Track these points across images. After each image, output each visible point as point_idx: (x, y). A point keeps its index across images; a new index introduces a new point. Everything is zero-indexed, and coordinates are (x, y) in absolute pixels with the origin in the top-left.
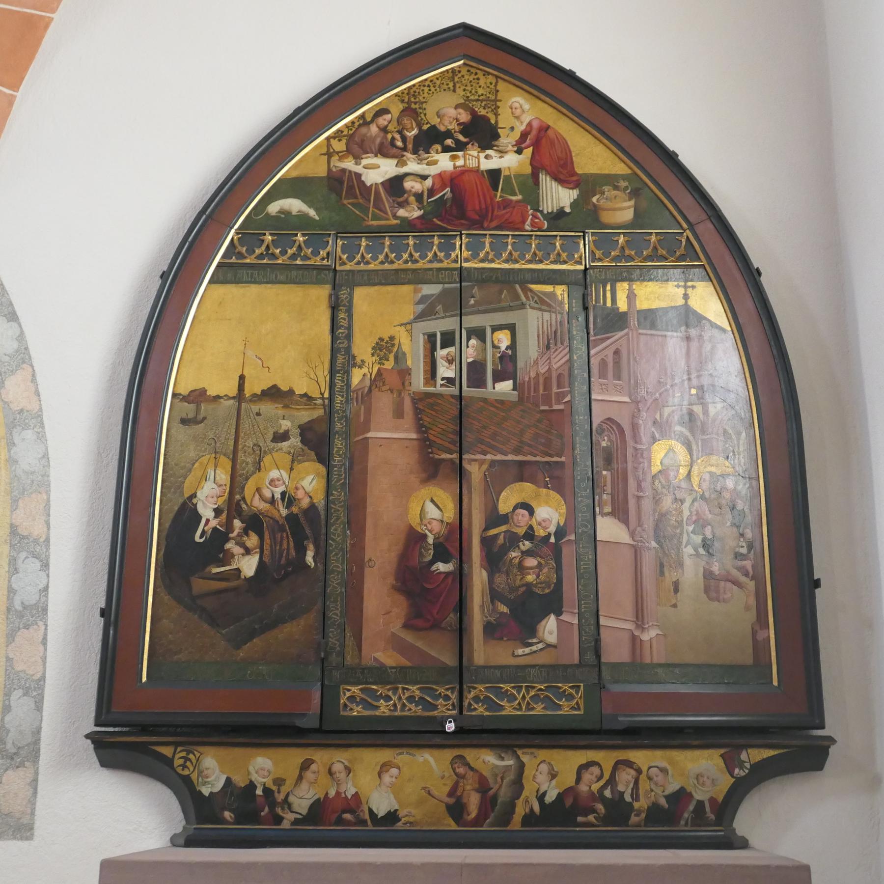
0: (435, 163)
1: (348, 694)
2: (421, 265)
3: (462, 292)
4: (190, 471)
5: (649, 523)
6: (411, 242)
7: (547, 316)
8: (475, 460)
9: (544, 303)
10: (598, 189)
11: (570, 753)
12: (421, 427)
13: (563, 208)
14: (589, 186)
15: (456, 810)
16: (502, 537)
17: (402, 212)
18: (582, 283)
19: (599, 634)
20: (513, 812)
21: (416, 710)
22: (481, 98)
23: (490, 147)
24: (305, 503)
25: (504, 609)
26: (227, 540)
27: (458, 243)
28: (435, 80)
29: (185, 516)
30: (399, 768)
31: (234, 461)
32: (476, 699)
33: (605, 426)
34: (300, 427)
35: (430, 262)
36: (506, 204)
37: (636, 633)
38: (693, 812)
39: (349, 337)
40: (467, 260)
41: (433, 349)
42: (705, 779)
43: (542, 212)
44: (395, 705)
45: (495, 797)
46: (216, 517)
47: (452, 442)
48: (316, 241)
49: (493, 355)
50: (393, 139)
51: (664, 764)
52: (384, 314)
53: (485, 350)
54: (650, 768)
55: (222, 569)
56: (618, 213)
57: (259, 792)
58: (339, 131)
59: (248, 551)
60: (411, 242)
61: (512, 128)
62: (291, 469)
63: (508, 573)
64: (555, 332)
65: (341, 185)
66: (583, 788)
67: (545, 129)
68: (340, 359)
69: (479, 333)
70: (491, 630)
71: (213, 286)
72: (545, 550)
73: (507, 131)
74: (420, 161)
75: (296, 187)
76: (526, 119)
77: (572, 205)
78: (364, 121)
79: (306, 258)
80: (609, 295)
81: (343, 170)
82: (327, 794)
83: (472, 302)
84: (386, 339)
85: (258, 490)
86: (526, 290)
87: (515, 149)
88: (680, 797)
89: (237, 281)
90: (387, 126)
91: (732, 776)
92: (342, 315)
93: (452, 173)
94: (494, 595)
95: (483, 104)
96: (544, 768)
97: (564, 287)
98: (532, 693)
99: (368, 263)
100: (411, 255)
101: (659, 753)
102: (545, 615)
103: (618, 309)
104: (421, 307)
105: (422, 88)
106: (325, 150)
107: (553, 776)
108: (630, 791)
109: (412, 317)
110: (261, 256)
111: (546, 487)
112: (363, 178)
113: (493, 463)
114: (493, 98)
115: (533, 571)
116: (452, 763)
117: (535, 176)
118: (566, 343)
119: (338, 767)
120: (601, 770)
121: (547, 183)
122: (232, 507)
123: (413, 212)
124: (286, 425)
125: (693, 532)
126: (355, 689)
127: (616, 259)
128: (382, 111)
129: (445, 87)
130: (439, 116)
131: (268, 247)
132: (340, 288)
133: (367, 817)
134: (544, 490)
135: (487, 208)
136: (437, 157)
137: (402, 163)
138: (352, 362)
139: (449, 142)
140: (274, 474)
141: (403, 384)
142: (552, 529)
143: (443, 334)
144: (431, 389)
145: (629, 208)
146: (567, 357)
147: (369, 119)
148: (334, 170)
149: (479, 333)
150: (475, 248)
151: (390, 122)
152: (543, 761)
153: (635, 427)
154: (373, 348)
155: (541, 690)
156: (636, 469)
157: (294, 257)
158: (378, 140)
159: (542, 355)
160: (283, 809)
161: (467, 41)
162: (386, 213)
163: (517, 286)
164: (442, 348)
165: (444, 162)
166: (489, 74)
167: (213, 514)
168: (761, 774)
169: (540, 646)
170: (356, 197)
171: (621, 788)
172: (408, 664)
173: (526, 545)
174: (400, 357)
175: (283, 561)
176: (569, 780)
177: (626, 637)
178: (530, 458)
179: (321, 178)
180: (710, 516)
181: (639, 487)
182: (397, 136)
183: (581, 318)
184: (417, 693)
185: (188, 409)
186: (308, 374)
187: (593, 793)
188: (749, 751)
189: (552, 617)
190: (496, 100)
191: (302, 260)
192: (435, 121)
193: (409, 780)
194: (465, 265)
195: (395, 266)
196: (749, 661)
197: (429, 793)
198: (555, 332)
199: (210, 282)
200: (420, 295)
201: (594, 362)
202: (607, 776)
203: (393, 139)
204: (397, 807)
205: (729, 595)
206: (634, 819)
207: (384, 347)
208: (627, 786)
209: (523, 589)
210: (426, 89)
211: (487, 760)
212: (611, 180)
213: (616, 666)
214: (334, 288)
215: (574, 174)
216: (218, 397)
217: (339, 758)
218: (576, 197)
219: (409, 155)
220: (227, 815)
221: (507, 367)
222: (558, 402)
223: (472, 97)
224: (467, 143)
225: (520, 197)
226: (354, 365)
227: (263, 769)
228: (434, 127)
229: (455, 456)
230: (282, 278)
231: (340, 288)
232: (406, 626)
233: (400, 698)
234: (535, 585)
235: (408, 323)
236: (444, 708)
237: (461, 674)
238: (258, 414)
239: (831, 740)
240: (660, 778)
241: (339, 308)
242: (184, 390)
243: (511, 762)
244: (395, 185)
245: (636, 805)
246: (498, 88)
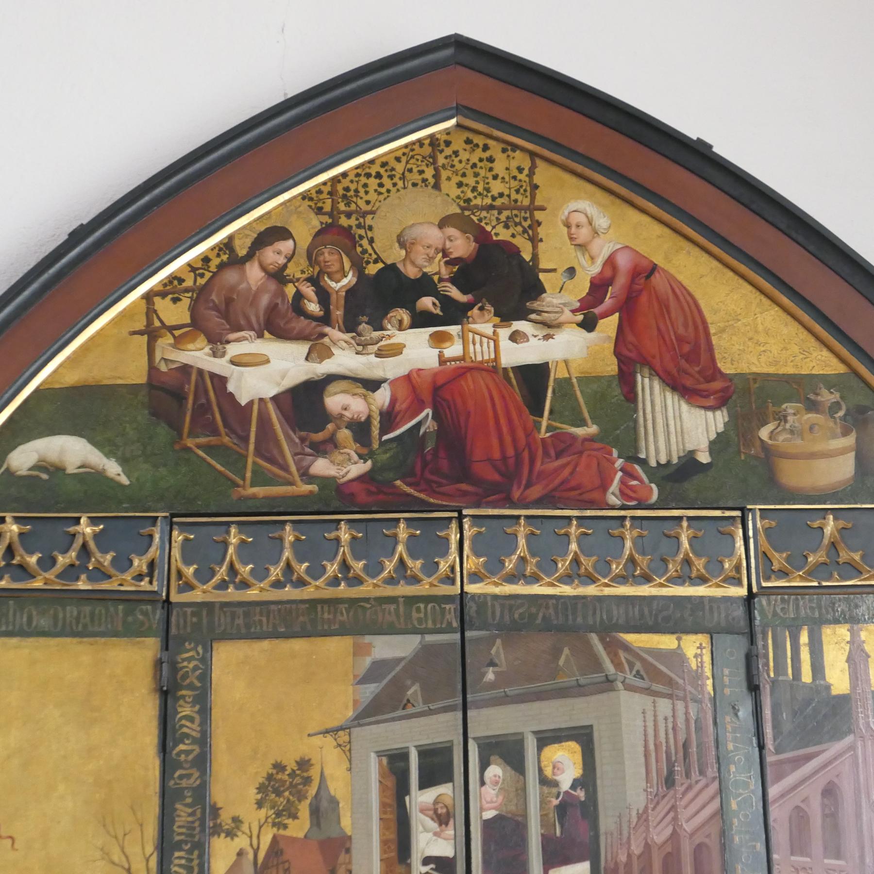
0: (396, 350)
2: (368, 589)
6: (345, 534)
7: (664, 706)
9: (659, 677)
10: (771, 408)
13: (692, 453)
14: (750, 400)
17: (321, 466)
22: (498, 202)
23: (522, 314)
27: (454, 538)
28: (393, 163)
35: (391, 581)
36: (563, 445)
39: (202, 762)
40: (476, 577)
41: (402, 789)
43: (644, 463)
49: (543, 802)
50: (299, 296)
53: (522, 791)
56: (821, 464)
58: (174, 278)
60: (345, 534)
61: (571, 272)
64: (686, 746)
65: (179, 405)
67: (645, 272)
68: (183, 814)
69: (507, 750)
74: (362, 346)
75: (75, 408)
76: (603, 249)
78: (231, 257)
79: (101, 574)
80: (805, 655)
81: (185, 369)
83: (490, 676)
84: (291, 765)
86: (614, 647)
87: (580, 317)
90: (285, 266)
92: (186, 710)
93: (436, 375)
95: (503, 217)
97: (703, 639)
99: (245, 585)
100: (345, 566)
103: (828, 687)
104: (371, 690)
105: (363, 180)
106: (141, 324)
109: (350, 714)
112: (231, 387)
114: (526, 202)
117: (626, 378)
118: (712, 772)
121: (653, 394)
123: (347, 466)
128: (273, 234)
129: (416, 177)
130: (402, 245)
132: (178, 645)
135: (518, 456)
137: (319, 351)
138: (210, 822)
139: (427, 303)
143: (425, 753)
145: (843, 452)
146: (715, 804)
147: (242, 252)
148: (163, 368)
149: (507, 750)
151: (290, 259)
154: (261, 789)
157: (71, 572)
158: (265, 300)
159: (657, 799)
162: (285, 468)
163: (594, 638)
164: (424, 784)
165: (417, 350)
166: (515, 147)
170: (215, 432)
174: (323, 811)
179: (134, 389)
182: (309, 290)
183: (745, 711)
186: (106, 854)
190: (532, 208)
191: (90, 579)
192: (395, 255)
194: (472, 588)
195: (308, 593)
198: (686, 746)
200: (368, 661)
203: (299, 296)
207: (285, 786)
210: (373, 183)
212: (800, 388)
214: (166, 647)
215: (715, 373)
218: (721, 428)
223: (478, 201)
224: (470, 306)
225: (592, 429)
226: (217, 830)
228: (392, 269)
230: (44, 623)
231: (178, 645)
235: (341, 728)
241: (177, 693)
244: (304, 403)
246: (537, 180)
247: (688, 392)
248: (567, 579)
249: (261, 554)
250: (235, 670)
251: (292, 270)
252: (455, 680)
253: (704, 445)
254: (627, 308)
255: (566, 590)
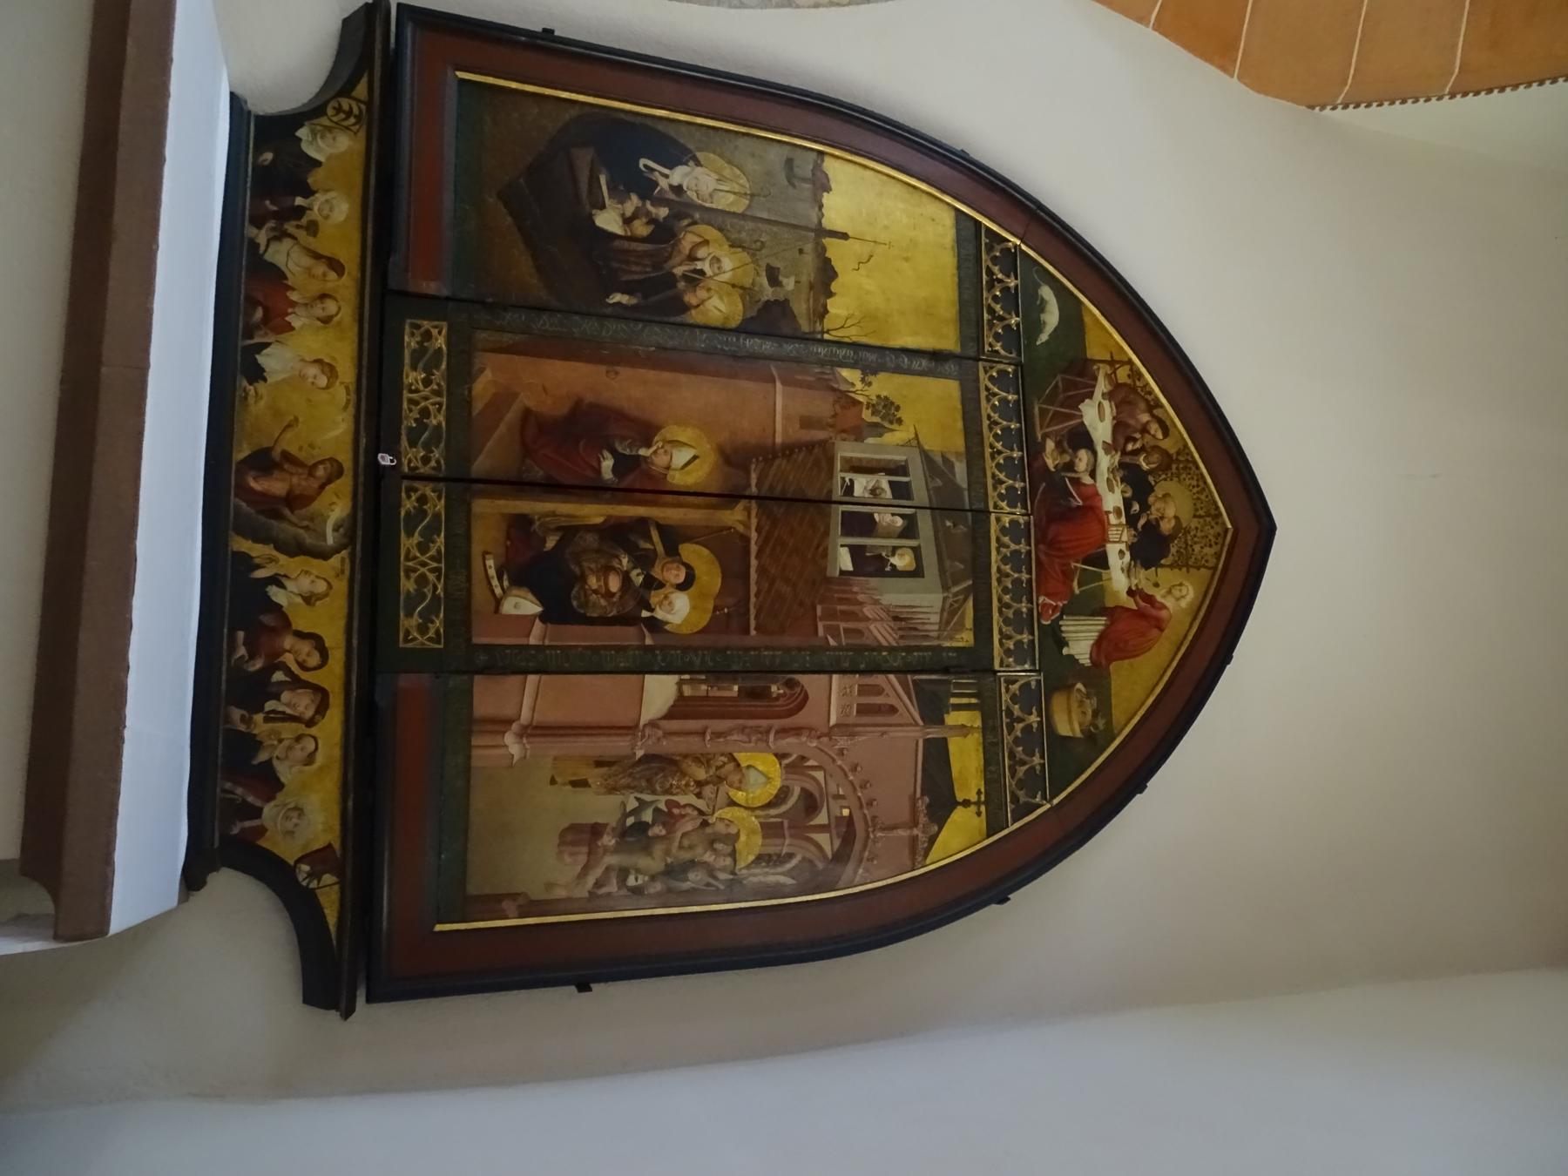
0: (1111, 489)
1: (435, 332)
2: (990, 466)
3: (959, 514)
4: (730, 162)
5: (668, 746)
7: (935, 618)
8: (749, 516)
9: (950, 613)
11: (342, 623)
12: (789, 450)
13: (1067, 644)
14: (1096, 676)
15: (264, 461)
16: (648, 546)
18: (975, 663)
19: (514, 673)
20: (256, 541)
21: (410, 420)
24: (690, 298)
25: (551, 543)
26: (643, 198)
29: (675, 154)
30: (327, 387)
31: (743, 216)
32: (423, 500)
33: (798, 690)
34: (787, 301)
35: (994, 476)
36: (1067, 575)
37: (515, 726)
38: (244, 801)
39: (898, 370)
40: (998, 520)
41: (889, 472)
42: (295, 820)
43: (1061, 618)
44: (417, 391)
45: (279, 516)
46: (671, 187)
47: (772, 488)
48: (1011, 338)
50: (1135, 440)
51: (320, 759)
52: (928, 413)
54: (315, 739)
55: (604, 188)
57: (299, 201)
58: (1140, 375)
59: (627, 221)
61: (1156, 585)
62: (734, 286)
63: (598, 551)
66: (288, 642)
68: (872, 357)
69: (909, 531)
70: (520, 525)
71: (953, 214)
72: (631, 604)
73: (1153, 579)
74: (1112, 471)
76: (1169, 602)
77: (1071, 657)
80: (965, 701)
82: (293, 289)
84: (899, 415)
85: (706, 242)
88: (270, 784)
89: (960, 241)
91: (300, 860)
92: (924, 363)
93: (1100, 508)
94: (570, 532)
96: (321, 587)
98: (431, 577)
99: (988, 400)
100: (999, 452)
101: (337, 752)
102: (540, 597)
104: (939, 459)
106: (1116, 358)
107: (309, 599)
108: (281, 708)
110: (990, 273)
111: (716, 608)
113: (747, 540)
115: (604, 584)
116: (331, 460)
117: (1103, 611)
118: (903, 643)
119: (331, 307)
120: (315, 669)
122: (683, 209)
124: (789, 283)
125: (657, 811)
126: (441, 342)
127: (1010, 713)
131: (1000, 281)
133: (256, 340)
134: (711, 606)
135: (1060, 549)
136: (1118, 490)
138: (869, 370)
139: (1136, 507)
140: (727, 264)
141: (844, 431)
142: (660, 614)
143: (907, 484)
144: (838, 465)
145: (1073, 730)
146: (885, 643)
147: (1155, 412)
149: (909, 531)
150: (1013, 531)
152: (330, 586)
153: (797, 731)
155: (435, 588)
156: (743, 729)
157: (991, 311)
158: (1132, 422)
159: (887, 610)
160: (273, 229)
161: (1253, 531)
165: (1112, 500)
166: (1218, 559)
167: (675, 184)
168: (299, 906)
169: (498, 591)
170: (1065, 391)
171: (286, 696)
172: (475, 412)
173: (638, 578)
174: (877, 430)
175: (615, 265)
176: (303, 620)
177: (508, 711)
178: (753, 589)
179: (1083, 348)
180: (679, 834)
181: (717, 735)
182: (1138, 445)
184: (434, 422)
185: (805, 166)
187: (279, 654)
188: (336, 887)
189: (538, 609)
192: (1159, 491)
193: (309, 400)
194: (993, 516)
196: (472, 889)
197: (289, 426)
199: (957, 210)
200: (953, 459)
201: (879, 679)
202: (304, 676)
203: (1135, 440)
204: (270, 380)
205: (568, 859)
206: (237, 713)
208: (288, 705)
209: (577, 570)
211: (335, 507)
213: (469, 692)
215: (1110, 660)
216: (821, 206)
217: (344, 307)
219: (1117, 457)
220: (269, 156)
221: (870, 564)
222: (827, 628)
225: (1077, 591)
226: (865, 373)
227: (331, 209)
228: (1151, 489)
229: (754, 490)
232: (527, 414)
233: (426, 398)
234: (582, 588)
236: (412, 456)
237: (461, 483)
238: (801, 251)
239: (348, 1012)
240: (298, 753)
242: (830, 166)
243: (330, 540)
244: (1081, 438)
245: (259, 717)
247: (1098, 644)
248: (999, 570)
249: (1004, 409)
250: (944, 391)
251: (1148, 438)
252: (943, 508)
253: (1072, 652)
254: (1139, 614)
255: (994, 569)
